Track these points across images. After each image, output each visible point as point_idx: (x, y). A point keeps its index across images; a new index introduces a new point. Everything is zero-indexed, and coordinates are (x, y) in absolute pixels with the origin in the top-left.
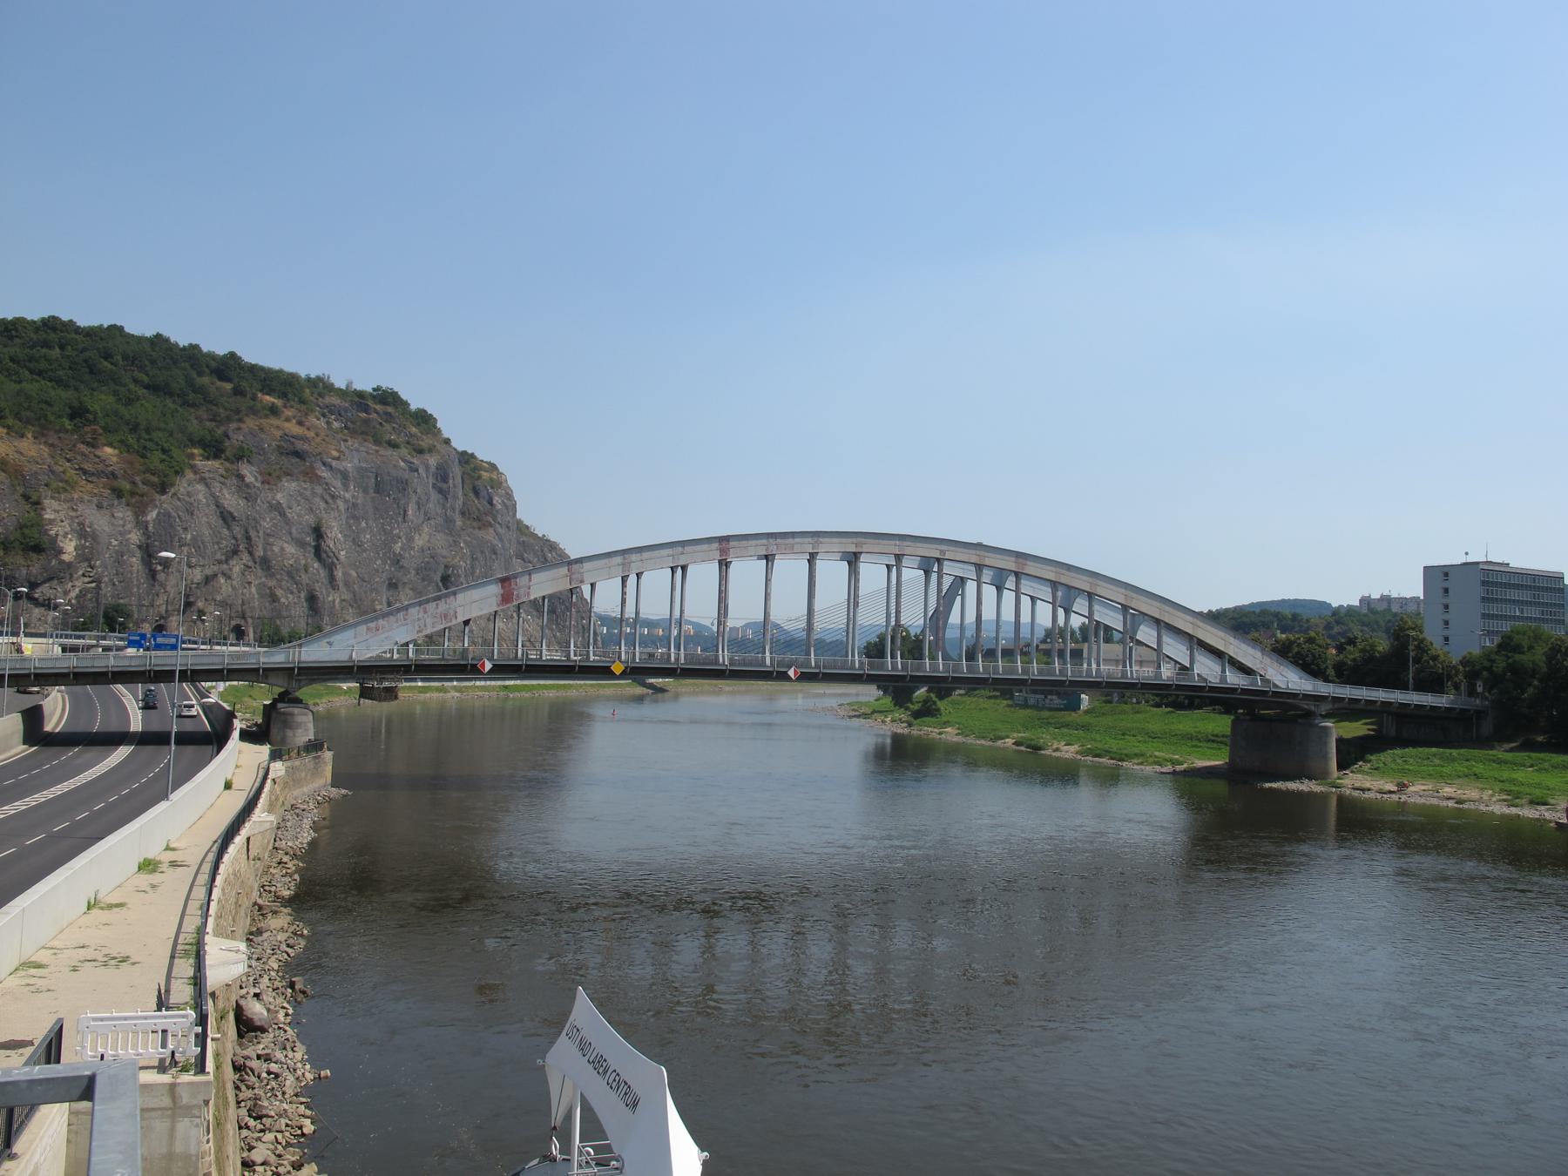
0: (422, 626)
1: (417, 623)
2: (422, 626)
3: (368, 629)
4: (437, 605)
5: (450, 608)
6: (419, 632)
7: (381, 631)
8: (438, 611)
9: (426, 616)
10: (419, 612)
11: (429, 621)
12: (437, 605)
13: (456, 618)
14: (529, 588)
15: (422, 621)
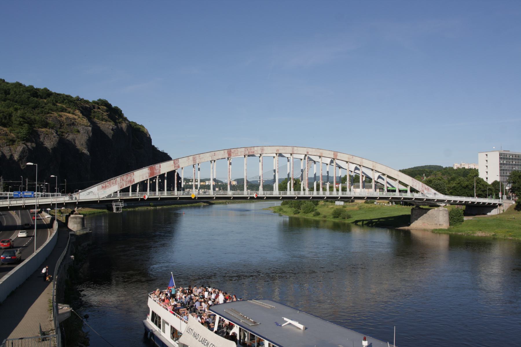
0: (122, 185)
1: (120, 184)
2: (122, 185)
3: (103, 187)
4: (127, 177)
5: (132, 178)
6: (121, 187)
7: (107, 188)
8: (128, 180)
9: (123, 181)
10: (121, 180)
11: (124, 183)
12: (127, 177)
13: (134, 182)
14: (160, 170)
15: (122, 183)
